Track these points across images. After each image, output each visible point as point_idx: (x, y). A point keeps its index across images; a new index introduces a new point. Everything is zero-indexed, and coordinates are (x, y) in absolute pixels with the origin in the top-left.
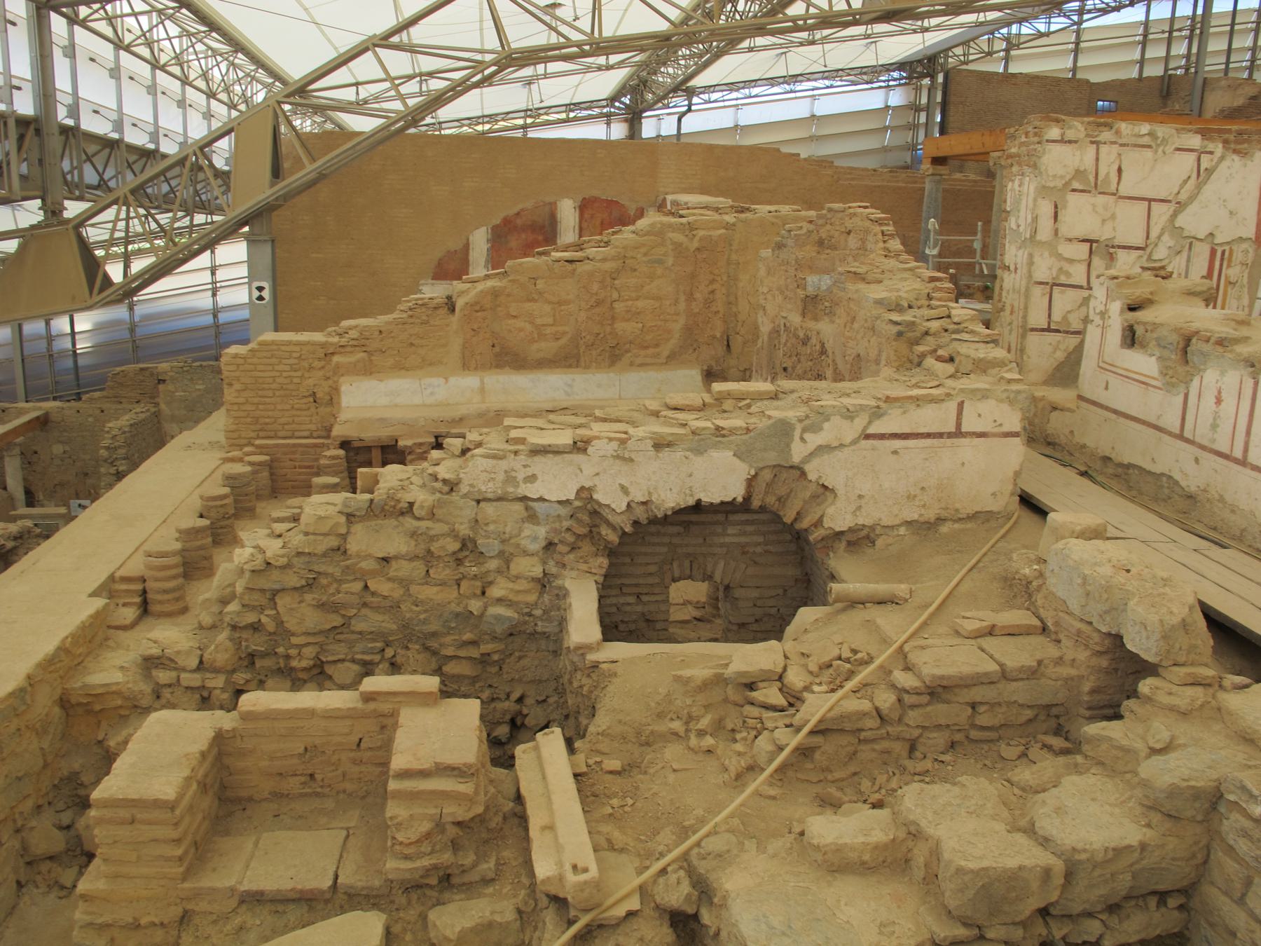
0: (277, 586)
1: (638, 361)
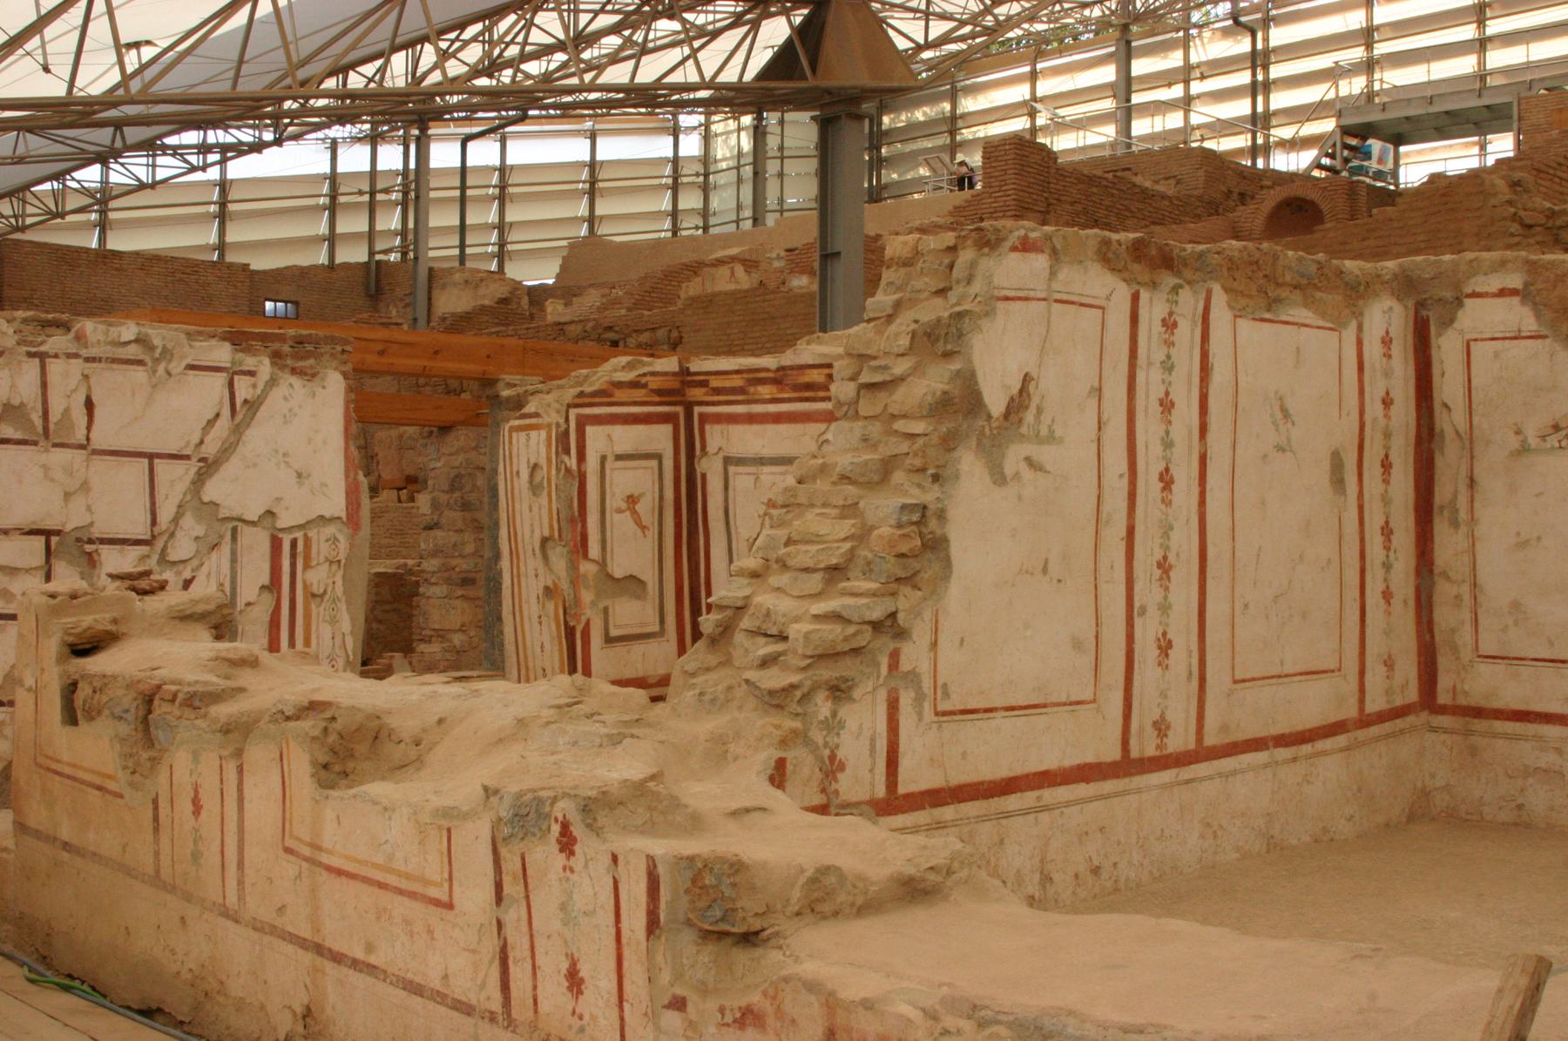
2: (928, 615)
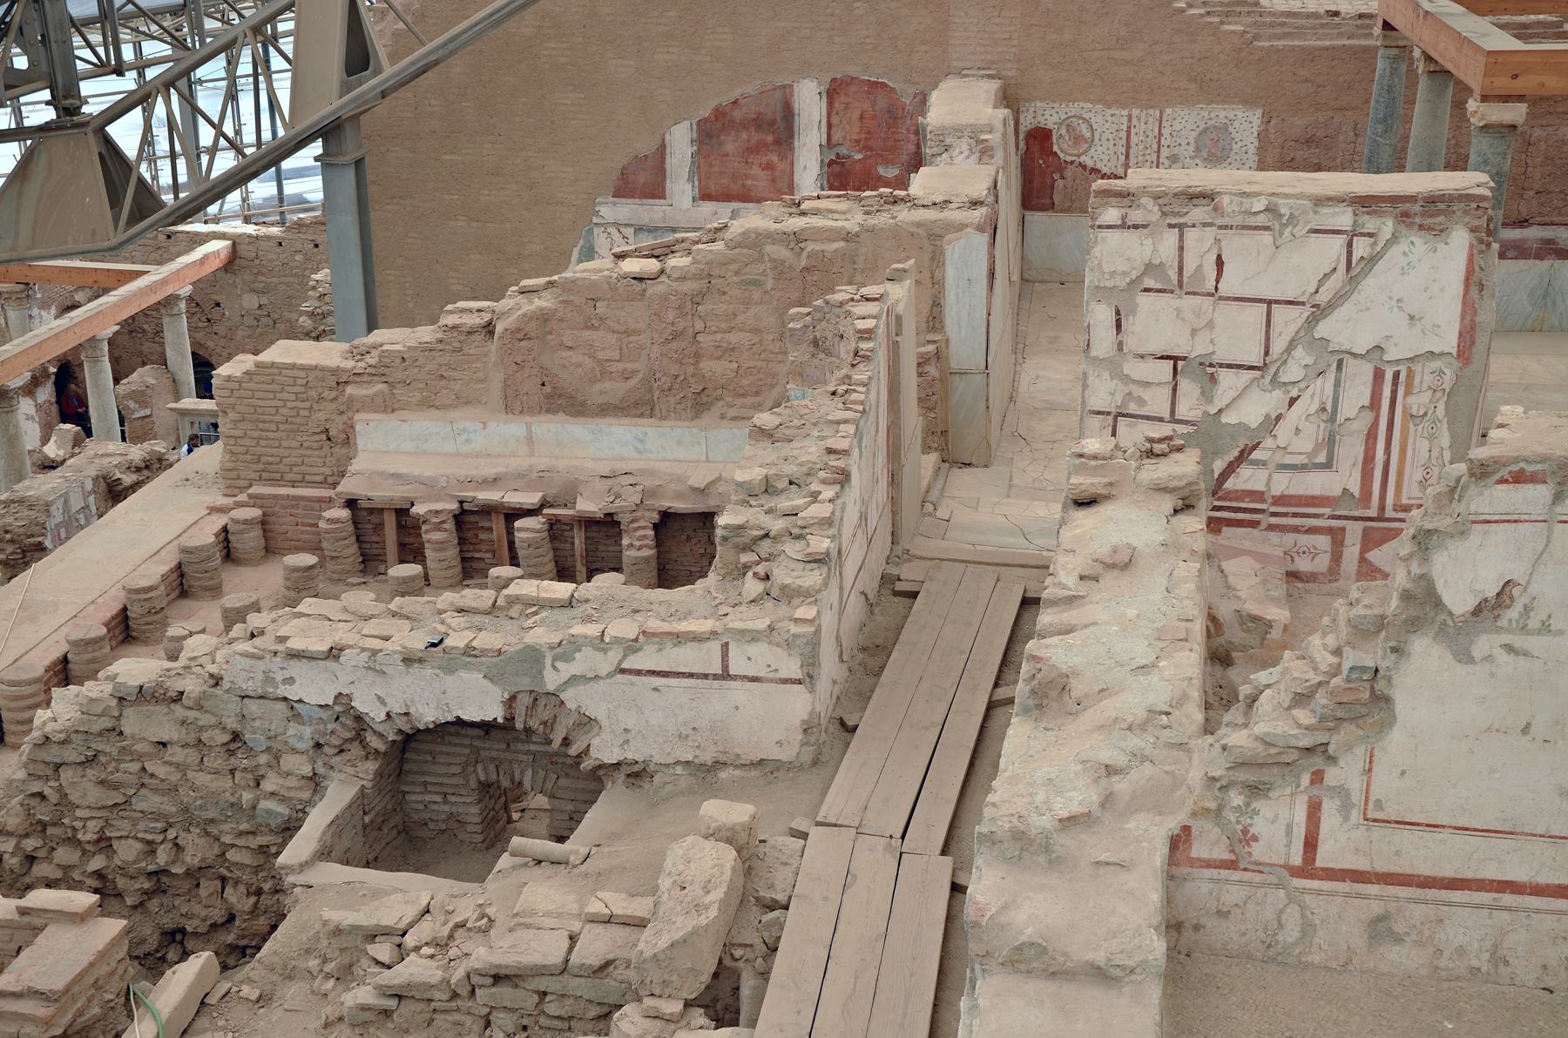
0: (58, 760)
1: (732, 413)
2: (1360, 751)
